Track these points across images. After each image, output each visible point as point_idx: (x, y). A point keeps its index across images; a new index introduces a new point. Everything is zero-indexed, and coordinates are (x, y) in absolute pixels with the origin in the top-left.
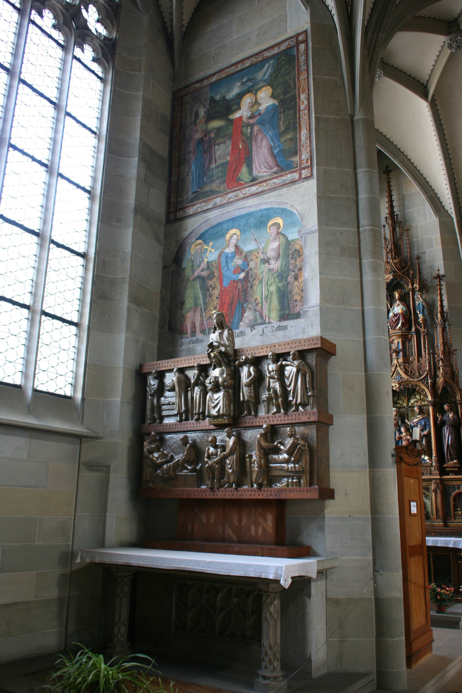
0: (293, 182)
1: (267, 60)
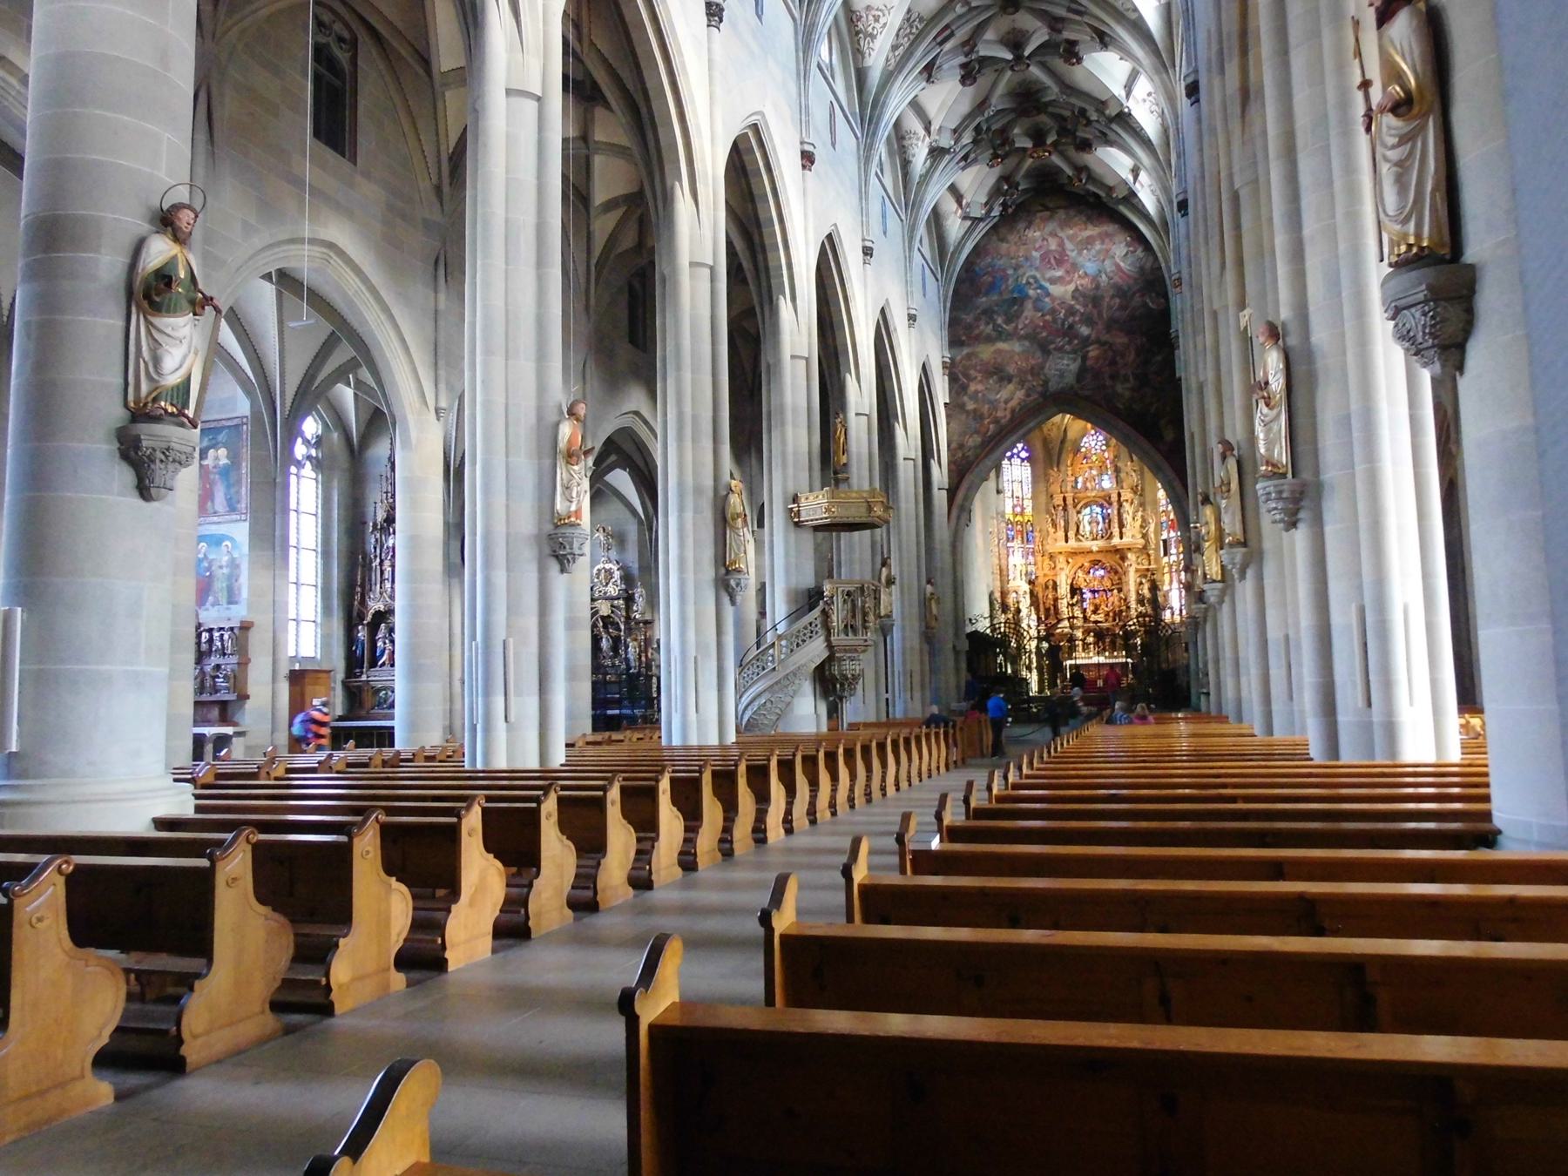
0: (237, 521)
1: (224, 428)
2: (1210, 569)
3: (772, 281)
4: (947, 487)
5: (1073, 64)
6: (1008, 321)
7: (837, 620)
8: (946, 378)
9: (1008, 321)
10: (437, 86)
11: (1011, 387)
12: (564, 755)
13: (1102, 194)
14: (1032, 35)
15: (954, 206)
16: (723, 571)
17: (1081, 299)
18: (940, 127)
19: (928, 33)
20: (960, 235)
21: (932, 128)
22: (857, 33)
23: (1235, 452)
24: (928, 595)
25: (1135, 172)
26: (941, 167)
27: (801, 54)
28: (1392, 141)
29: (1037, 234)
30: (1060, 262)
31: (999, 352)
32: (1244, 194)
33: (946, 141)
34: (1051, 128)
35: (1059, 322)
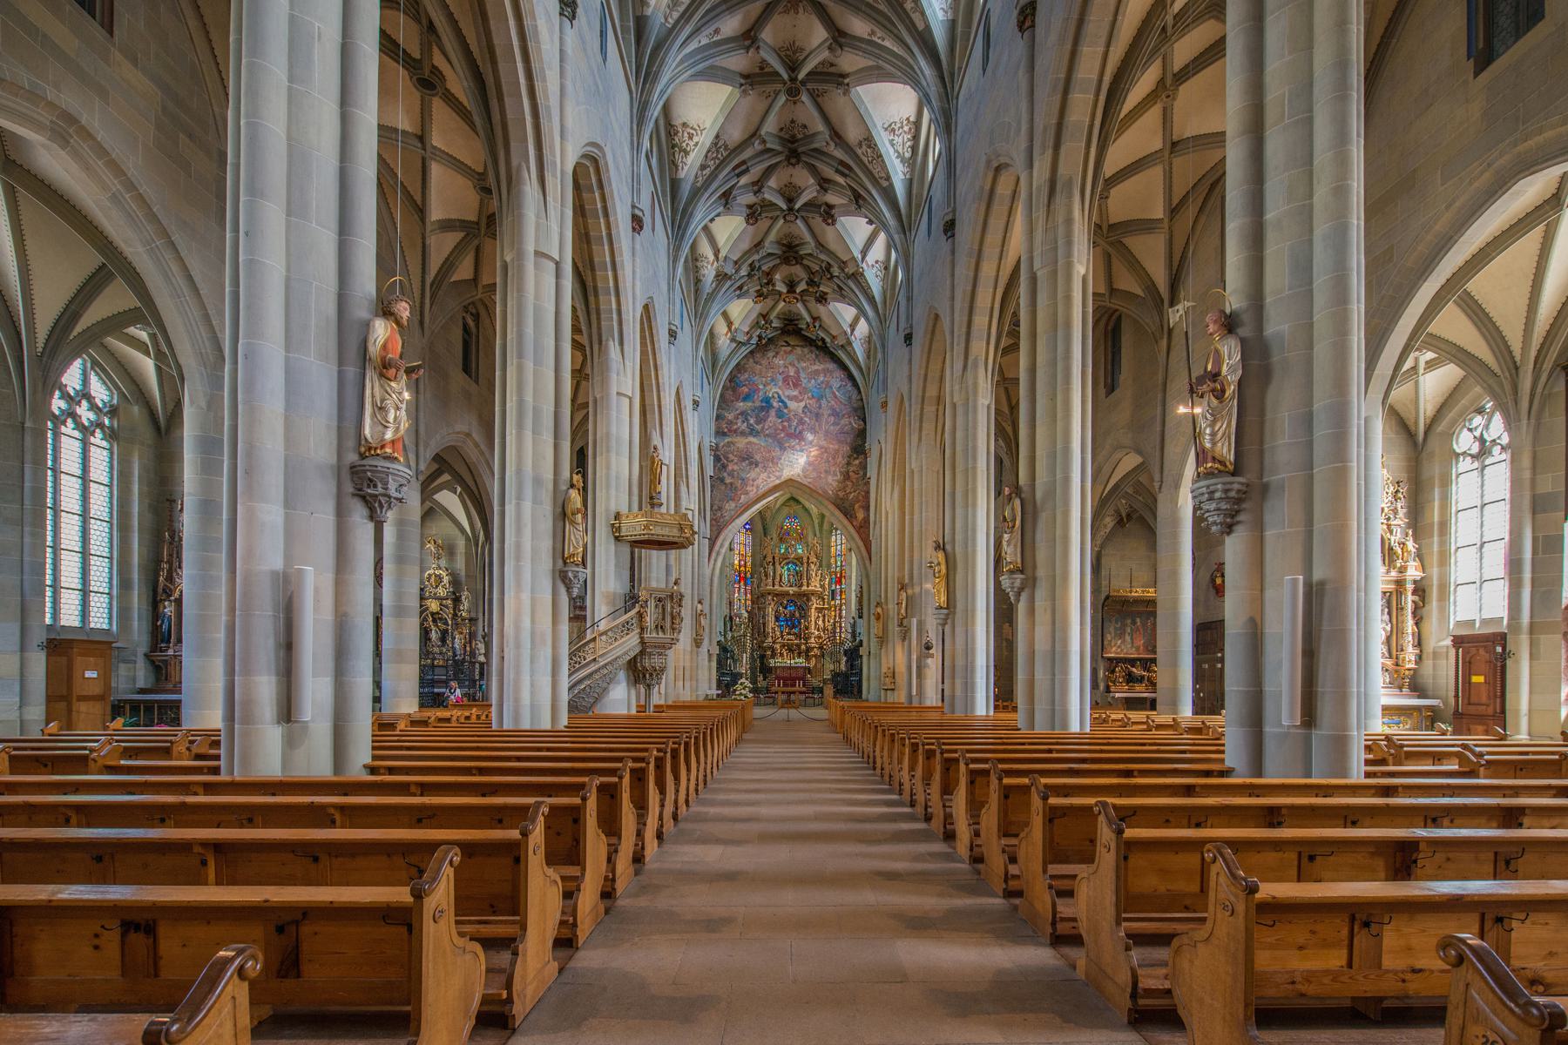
3: (603, 323)
6: (758, 423)
7: (650, 619)
9: (758, 423)
11: (757, 470)
14: (803, 191)
18: (726, 257)
31: (750, 443)
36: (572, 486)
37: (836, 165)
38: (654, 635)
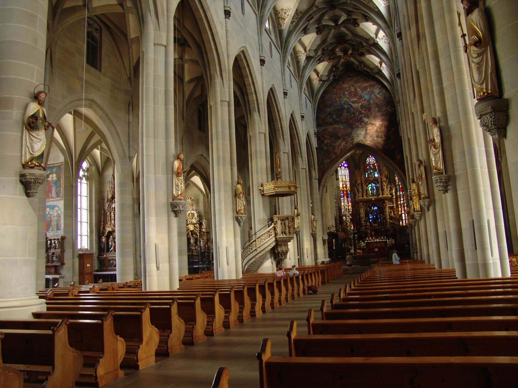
0: (59, 200)
1: (55, 167)
2: (416, 207)
3: (251, 106)
4: (318, 178)
5: (356, 27)
7: (279, 230)
8: (316, 138)
10: (129, 43)
11: (340, 141)
12: (178, 284)
13: (370, 71)
15: (316, 76)
16: (235, 213)
17: (364, 108)
18: (310, 49)
19: (304, 17)
20: (319, 87)
21: (307, 50)
22: (278, 18)
23: (423, 164)
24: (312, 219)
25: (381, 64)
26: (311, 63)
27: (259, 26)
28: (475, 55)
29: (347, 86)
30: (355, 96)
31: (335, 128)
32: (421, 71)
33: (312, 54)
34: (349, 49)
35: (356, 117)
36: (238, 183)
37: (353, 6)
38: (282, 236)
